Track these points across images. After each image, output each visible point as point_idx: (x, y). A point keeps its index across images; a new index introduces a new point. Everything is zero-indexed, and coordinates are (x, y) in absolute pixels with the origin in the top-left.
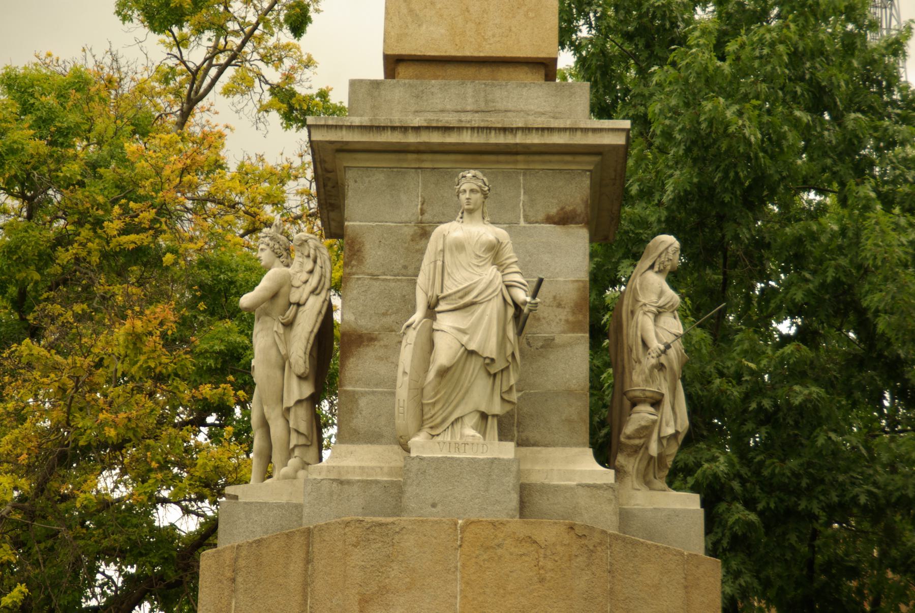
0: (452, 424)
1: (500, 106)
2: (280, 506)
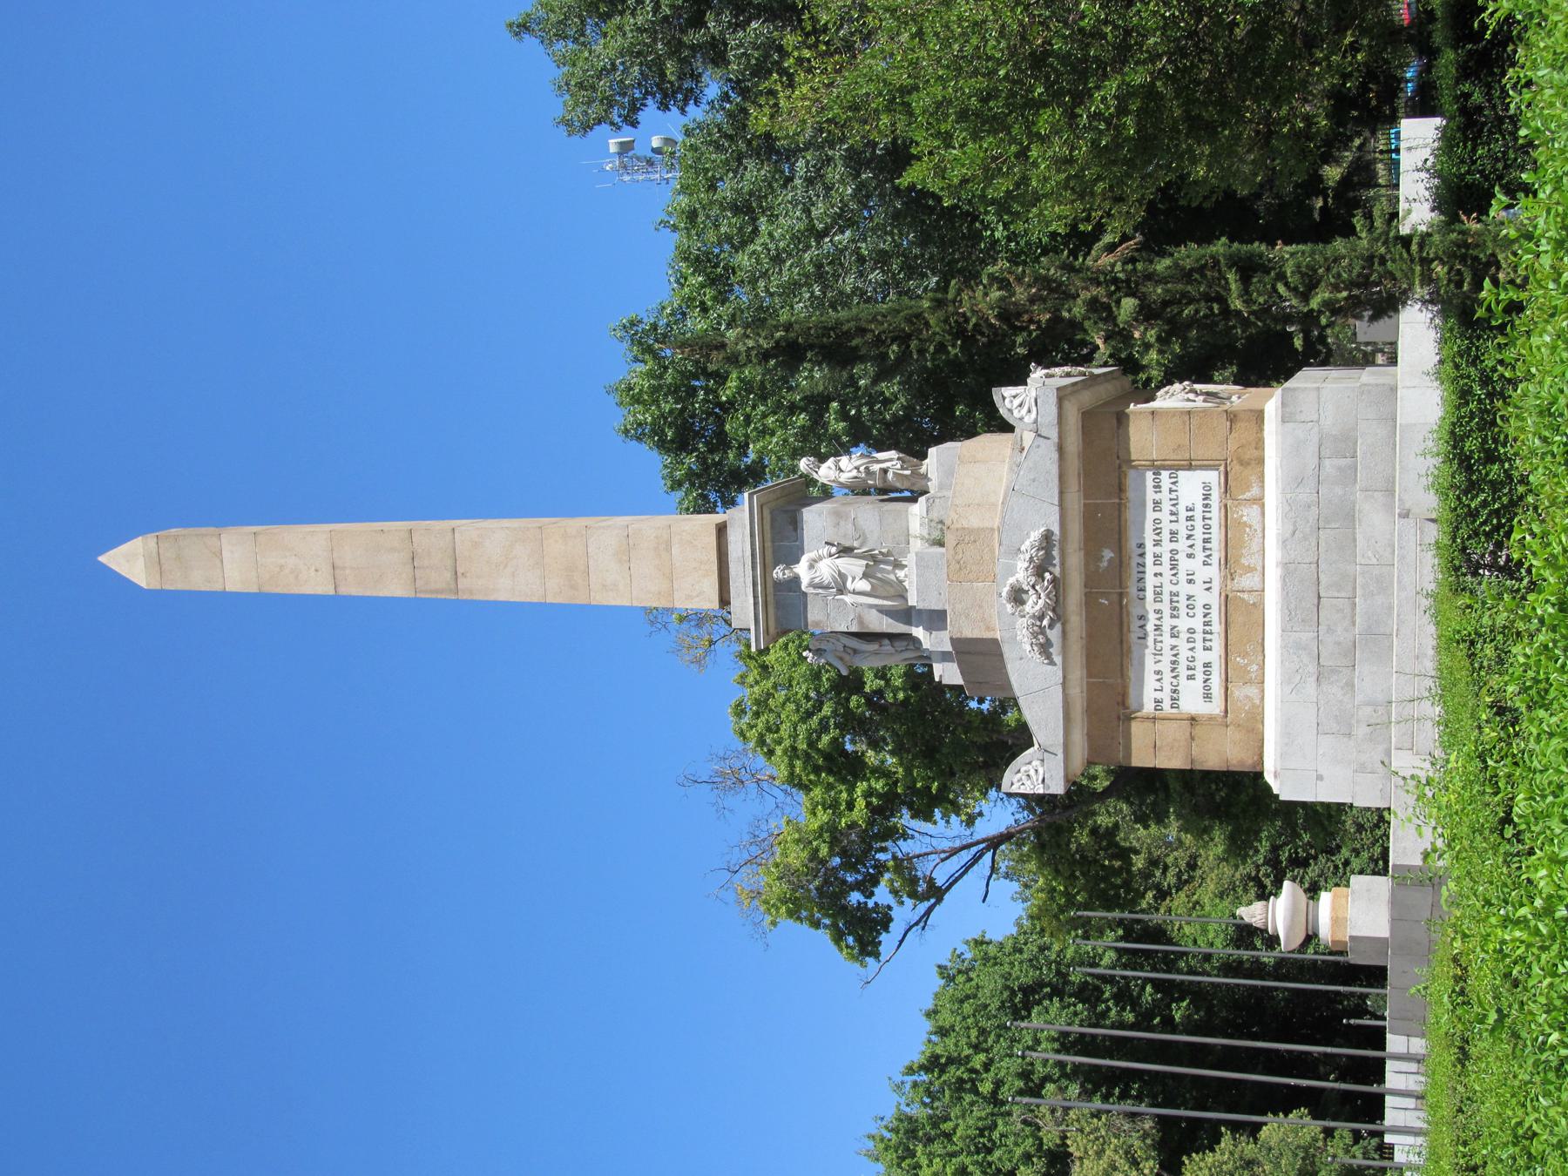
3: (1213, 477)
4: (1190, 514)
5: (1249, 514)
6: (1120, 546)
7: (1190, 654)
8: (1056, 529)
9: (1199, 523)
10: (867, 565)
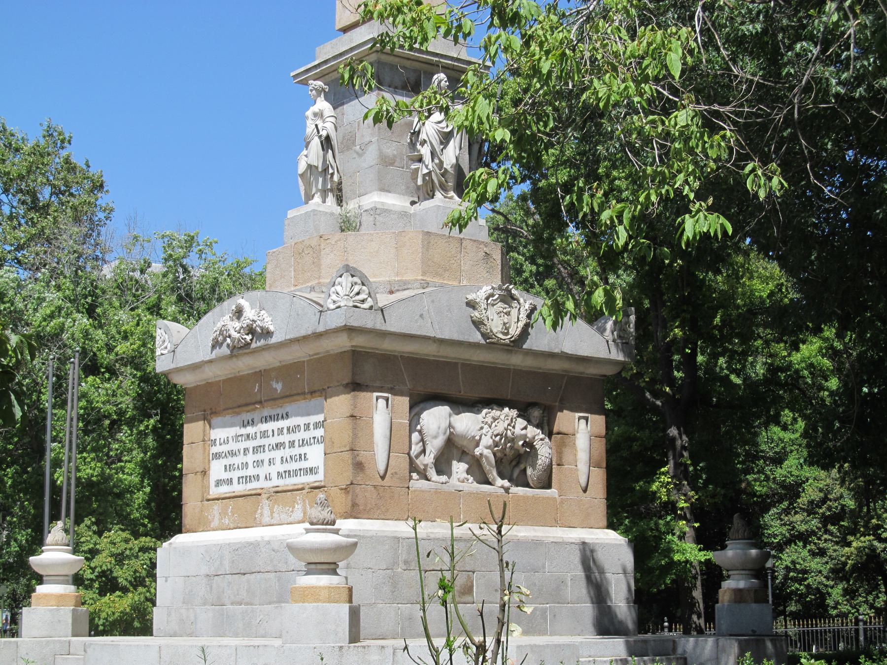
6: (289, 396)
8: (274, 340)
10: (317, 168)
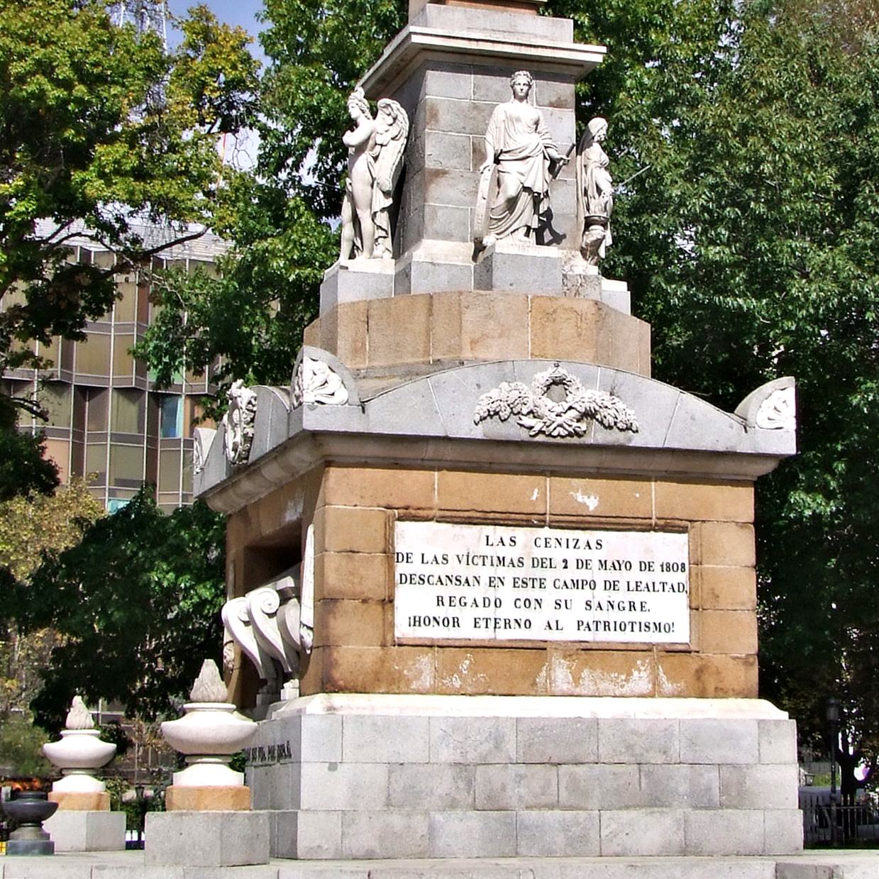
0: (512, 233)
1: (520, 29)
2: (374, 274)
3: (681, 635)
4: (638, 606)
5: (640, 679)
7: (470, 601)
8: (637, 441)
9: (627, 616)
